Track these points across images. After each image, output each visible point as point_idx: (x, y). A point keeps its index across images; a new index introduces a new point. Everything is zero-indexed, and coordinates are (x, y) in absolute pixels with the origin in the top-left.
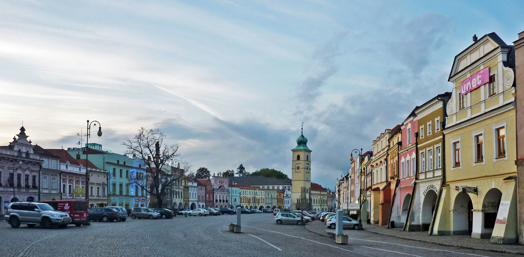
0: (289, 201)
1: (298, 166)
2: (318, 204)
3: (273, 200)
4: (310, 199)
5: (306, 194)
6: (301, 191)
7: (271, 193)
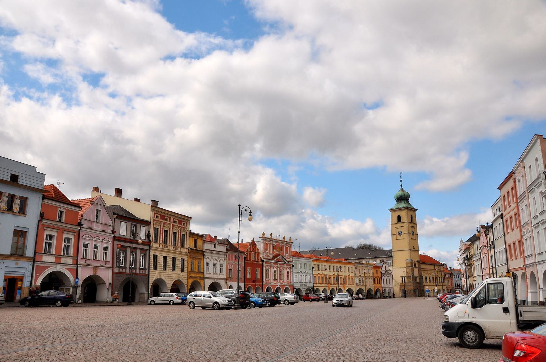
0: (389, 279)
1: (400, 231)
2: (432, 284)
3: (368, 280)
4: (421, 277)
5: (414, 268)
7: (364, 268)
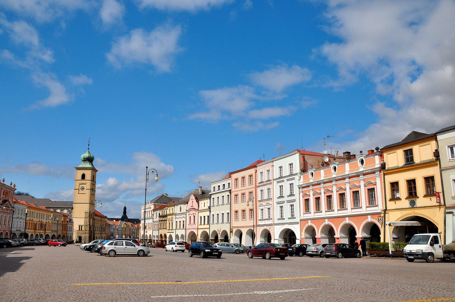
2: (98, 231)
4: (94, 225)
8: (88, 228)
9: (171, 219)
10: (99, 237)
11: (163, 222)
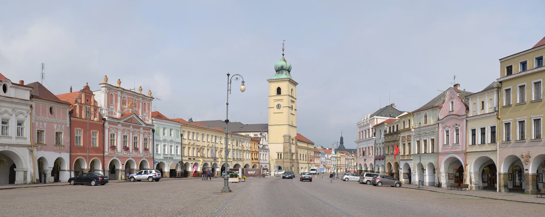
4: (297, 153)
6: (284, 140)
7: (242, 140)
8: (289, 156)
9: (406, 138)
10: (306, 167)
11: (393, 143)
